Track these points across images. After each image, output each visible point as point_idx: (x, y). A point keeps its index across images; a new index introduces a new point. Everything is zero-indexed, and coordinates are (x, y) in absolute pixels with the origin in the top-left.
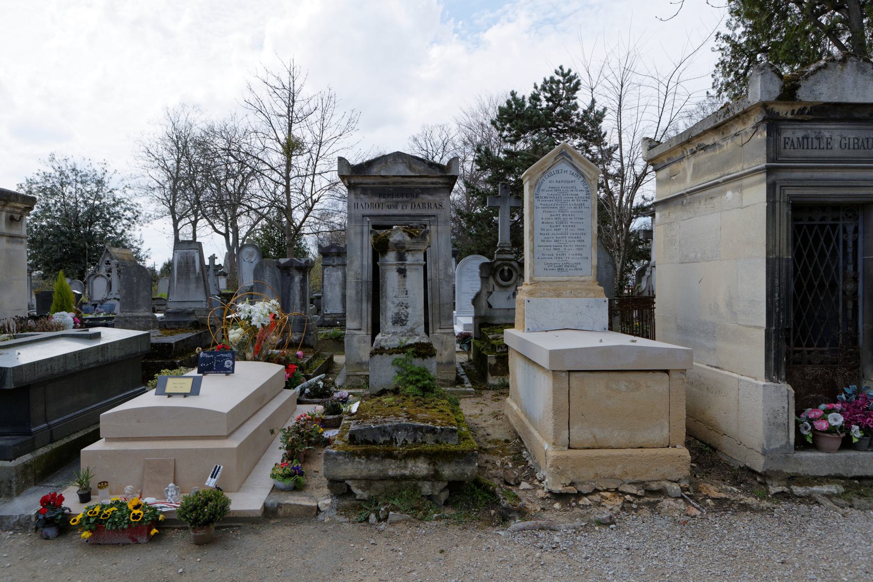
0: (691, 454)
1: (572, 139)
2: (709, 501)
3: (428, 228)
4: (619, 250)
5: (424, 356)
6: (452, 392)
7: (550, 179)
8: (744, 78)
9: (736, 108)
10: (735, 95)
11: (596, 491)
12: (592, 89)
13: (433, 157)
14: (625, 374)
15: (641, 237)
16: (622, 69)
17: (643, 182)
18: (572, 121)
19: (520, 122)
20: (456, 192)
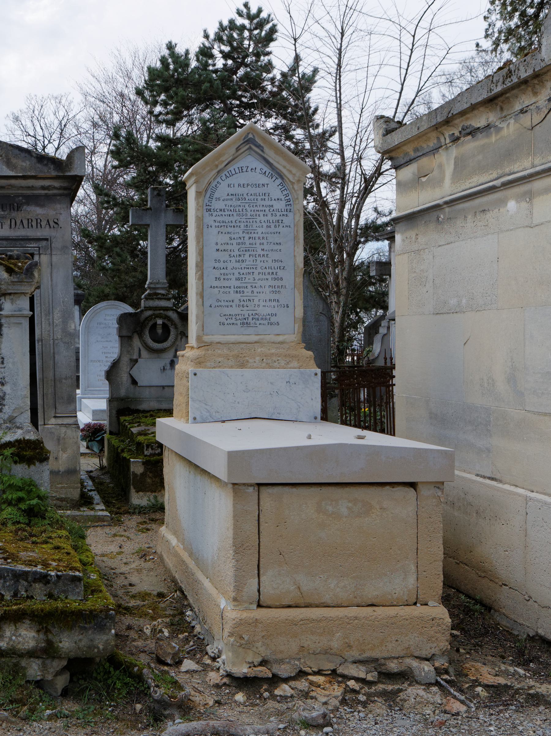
0: (452, 615)
1: (263, 118)
2: (479, 689)
3: (36, 258)
4: (338, 293)
5: (30, 461)
6: (74, 518)
7: (229, 181)
8: (535, 22)
9: (522, 68)
10: (521, 49)
11: (301, 674)
12: (295, 40)
13: (44, 147)
14: (347, 490)
15: (373, 273)
16: (343, 8)
17: (376, 186)
18: (264, 90)
19: (181, 92)
20: (81, 202)
